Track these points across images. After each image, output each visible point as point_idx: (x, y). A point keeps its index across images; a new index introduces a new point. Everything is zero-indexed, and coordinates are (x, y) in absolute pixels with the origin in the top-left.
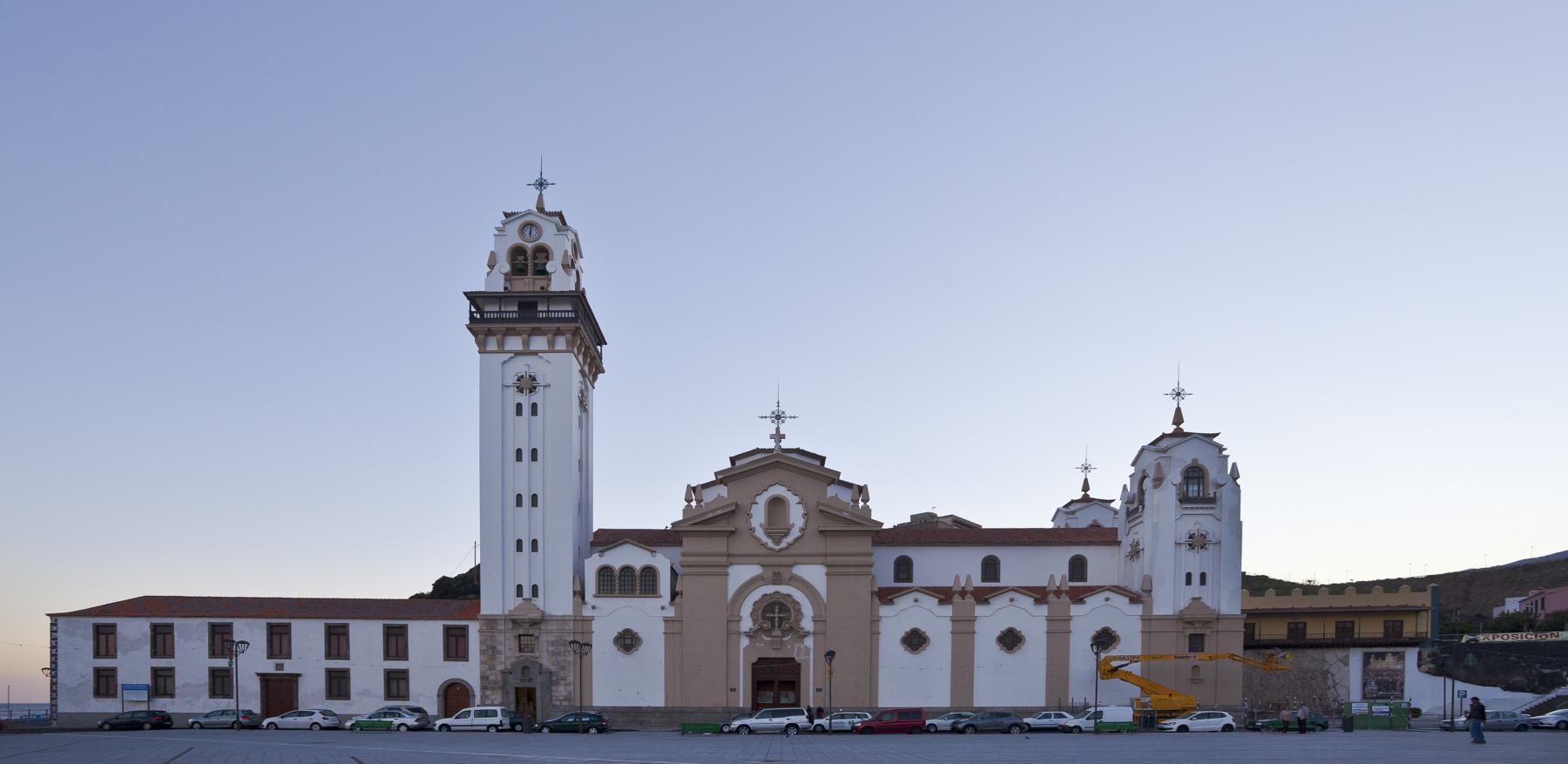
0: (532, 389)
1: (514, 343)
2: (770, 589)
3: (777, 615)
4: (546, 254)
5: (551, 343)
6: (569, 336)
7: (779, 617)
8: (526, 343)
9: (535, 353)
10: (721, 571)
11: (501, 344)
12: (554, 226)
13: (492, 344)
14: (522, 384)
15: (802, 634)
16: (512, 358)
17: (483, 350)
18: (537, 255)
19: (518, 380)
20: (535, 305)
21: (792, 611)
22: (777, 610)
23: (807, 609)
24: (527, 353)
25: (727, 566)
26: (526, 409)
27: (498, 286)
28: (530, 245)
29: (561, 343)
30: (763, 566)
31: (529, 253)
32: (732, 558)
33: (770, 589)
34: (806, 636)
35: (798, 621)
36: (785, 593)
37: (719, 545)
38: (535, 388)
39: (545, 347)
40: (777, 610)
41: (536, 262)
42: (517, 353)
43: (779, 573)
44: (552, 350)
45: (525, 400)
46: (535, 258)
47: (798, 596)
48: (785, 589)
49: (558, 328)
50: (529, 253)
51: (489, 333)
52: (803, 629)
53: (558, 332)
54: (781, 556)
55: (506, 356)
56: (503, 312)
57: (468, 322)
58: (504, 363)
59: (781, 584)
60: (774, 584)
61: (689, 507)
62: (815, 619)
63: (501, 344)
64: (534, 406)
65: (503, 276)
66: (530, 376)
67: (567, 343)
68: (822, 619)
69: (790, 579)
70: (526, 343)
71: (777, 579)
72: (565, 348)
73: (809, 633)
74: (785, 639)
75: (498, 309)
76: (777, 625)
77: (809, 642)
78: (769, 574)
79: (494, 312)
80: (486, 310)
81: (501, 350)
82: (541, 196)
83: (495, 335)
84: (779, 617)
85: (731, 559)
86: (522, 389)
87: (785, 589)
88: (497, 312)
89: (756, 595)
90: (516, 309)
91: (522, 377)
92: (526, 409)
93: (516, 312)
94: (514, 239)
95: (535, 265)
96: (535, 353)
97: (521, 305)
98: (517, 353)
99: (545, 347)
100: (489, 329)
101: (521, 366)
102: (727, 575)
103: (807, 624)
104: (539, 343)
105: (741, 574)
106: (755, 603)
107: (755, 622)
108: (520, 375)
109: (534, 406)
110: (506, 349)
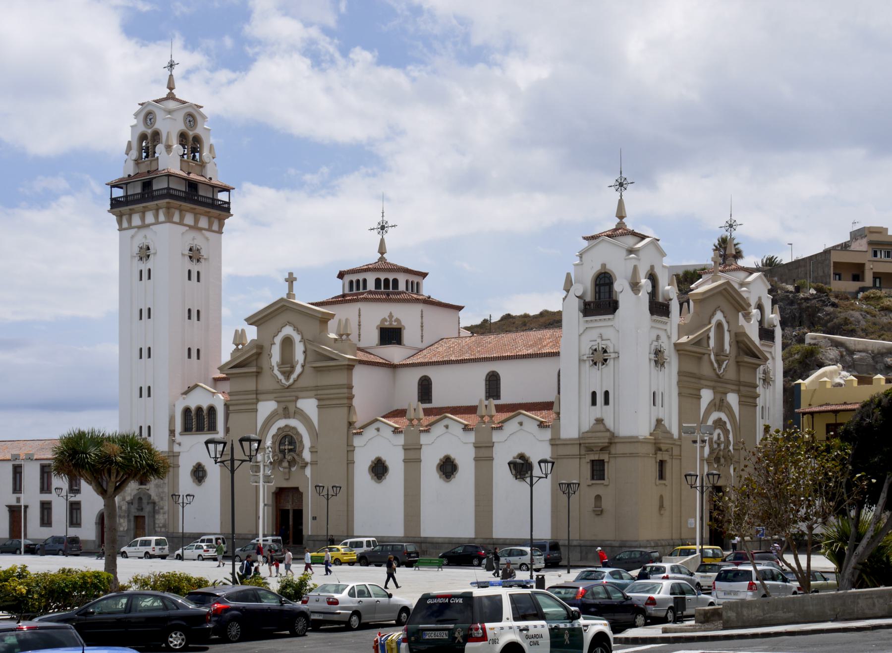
1: (136, 220)
2: (282, 423)
5: (156, 216)
7: (288, 445)
8: (143, 218)
9: (149, 226)
17: (120, 229)
22: (287, 443)
23: (307, 442)
24: (144, 226)
26: (145, 275)
29: (162, 218)
32: (258, 395)
33: (282, 423)
34: (305, 466)
35: (302, 451)
37: (250, 385)
38: (148, 256)
40: (287, 443)
42: (139, 227)
44: (157, 223)
45: (144, 266)
48: (293, 422)
52: (304, 459)
55: (132, 232)
57: (109, 208)
59: (289, 418)
60: (285, 418)
61: (237, 350)
69: (295, 413)
70: (143, 218)
71: (286, 413)
73: (307, 464)
74: (293, 469)
77: (308, 471)
78: (281, 411)
81: (130, 227)
85: (260, 397)
87: (293, 422)
89: (273, 431)
92: (145, 275)
98: (139, 227)
101: (140, 239)
102: (256, 410)
103: (307, 455)
104: (150, 218)
105: (266, 408)
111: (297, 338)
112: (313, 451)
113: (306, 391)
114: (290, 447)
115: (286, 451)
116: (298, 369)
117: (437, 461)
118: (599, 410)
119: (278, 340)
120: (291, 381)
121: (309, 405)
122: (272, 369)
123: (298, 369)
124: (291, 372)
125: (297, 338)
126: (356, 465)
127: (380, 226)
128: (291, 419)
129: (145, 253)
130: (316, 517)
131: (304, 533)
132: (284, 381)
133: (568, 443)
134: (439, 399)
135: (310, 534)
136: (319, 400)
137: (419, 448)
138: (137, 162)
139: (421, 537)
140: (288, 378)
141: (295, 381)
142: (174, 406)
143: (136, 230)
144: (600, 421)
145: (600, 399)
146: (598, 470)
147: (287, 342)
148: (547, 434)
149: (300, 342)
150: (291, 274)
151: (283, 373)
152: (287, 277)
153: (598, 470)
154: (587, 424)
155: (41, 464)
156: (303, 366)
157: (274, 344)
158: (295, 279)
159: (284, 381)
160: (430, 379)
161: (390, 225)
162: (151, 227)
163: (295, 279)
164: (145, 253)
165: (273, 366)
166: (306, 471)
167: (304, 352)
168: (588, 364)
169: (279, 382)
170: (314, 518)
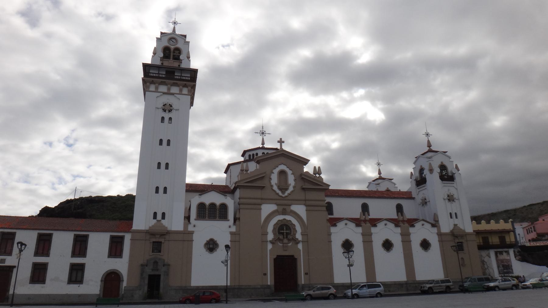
0: (170, 111)
1: (163, 88)
2: (281, 217)
3: (285, 231)
4: (179, 52)
5: (181, 90)
6: (190, 88)
8: (169, 89)
10: (257, 207)
11: (157, 88)
12: (184, 41)
13: (152, 87)
14: (166, 108)
15: (297, 242)
16: (161, 95)
18: (175, 51)
19: (164, 106)
20: (174, 72)
21: (292, 230)
22: (285, 229)
24: (168, 93)
25: (261, 205)
26: (166, 120)
27: (158, 63)
28: (172, 47)
30: (278, 205)
31: (172, 50)
33: (281, 217)
35: (295, 234)
36: (288, 220)
37: (257, 193)
39: (178, 92)
40: (285, 229)
41: (174, 54)
42: (164, 93)
43: (285, 209)
45: (167, 116)
46: (174, 52)
47: (294, 221)
48: (288, 218)
49: (185, 84)
50: (172, 50)
51: (152, 83)
53: (185, 86)
54: (286, 200)
55: (159, 94)
56: (160, 74)
58: (158, 97)
60: (283, 214)
62: (303, 234)
63: (157, 88)
64: (170, 119)
65: (160, 58)
66: (170, 105)
67: (189, 91)
68: (306, 234)
70: (169, 89)
71: (284, 212)
72: (187, 93)
73: (300, 241)
75: (158, 73)
76: (285, 237)
77: (300, 246)
79: (156, 74)
80: (151, 72)
81: (156, 91)
82: (174, 28)
83: (155, 84)
84: (286, 230)
86: (166, 110)
87: (288, 218)
88: (157, 74)
90: (165, 73)
91: (166, 104)
92: (166, 120)
93: (164, 74)
94: (165, 43)
95: (174, 56)
96: (173, 94)
97: (167, 72)
98: (164, 93)
99: (178, 92)
100: (153, 81)
102: (261, 209)
103: (299, 236)
104: (175, 90)
105: (267, 209)
106: (275, 225)
107: (274, 234)
108: (165, 103)
109: (170, 119)
110: (159, 90)
111: (289, 172)
112: (302, 234)
113: (298, 201)
114: (287, 232)
115: (285, 234)
116: (291, 189)
117: (381, 242)
118: (456, 221)
119: (276, 171)
120: (286, 194)
121: (300, 209)
122: (272, 186)
123: (291, 189)
124: (287, 189)
125: (289, 172)
126: (332, 243)
127: (264, 132)
128: (287, 216)
129: (167, 108)
130: (307, 273)
131: (299, 283)
132: (280, 194)
133: (445, 234)
134: (337, 214)
135: (303, 283)
136: (306, 206)
137: (371, 235)
138: (162, 59)
139: (416, 281)
140: (283, 193)
141: (289, 194)
142: (190, 201)
143: (162, 94)
144: (455, 225)
145: (454, 216)
146: (459, 247)
147: (282, 173)
148: (435, 230)
149: (292, 174)
150: (281, 139)
151: (280, 189)
152: (283, 140)
153: (459, 247)
154: (452, 227)
155: (38, 233)
156: (294, 187)
157: (274, 173)
158: (283, 142)
159: (280, 194)
160: (331, 203)
161: (267, 133)
162: (175, 95)
163: (283, 142)
164: (167, 108)
165: (273, 185)
166: (298, 246)
167: (295, 180)
168: (447, 201)
169: (278, 194)
170: (306, 274)
